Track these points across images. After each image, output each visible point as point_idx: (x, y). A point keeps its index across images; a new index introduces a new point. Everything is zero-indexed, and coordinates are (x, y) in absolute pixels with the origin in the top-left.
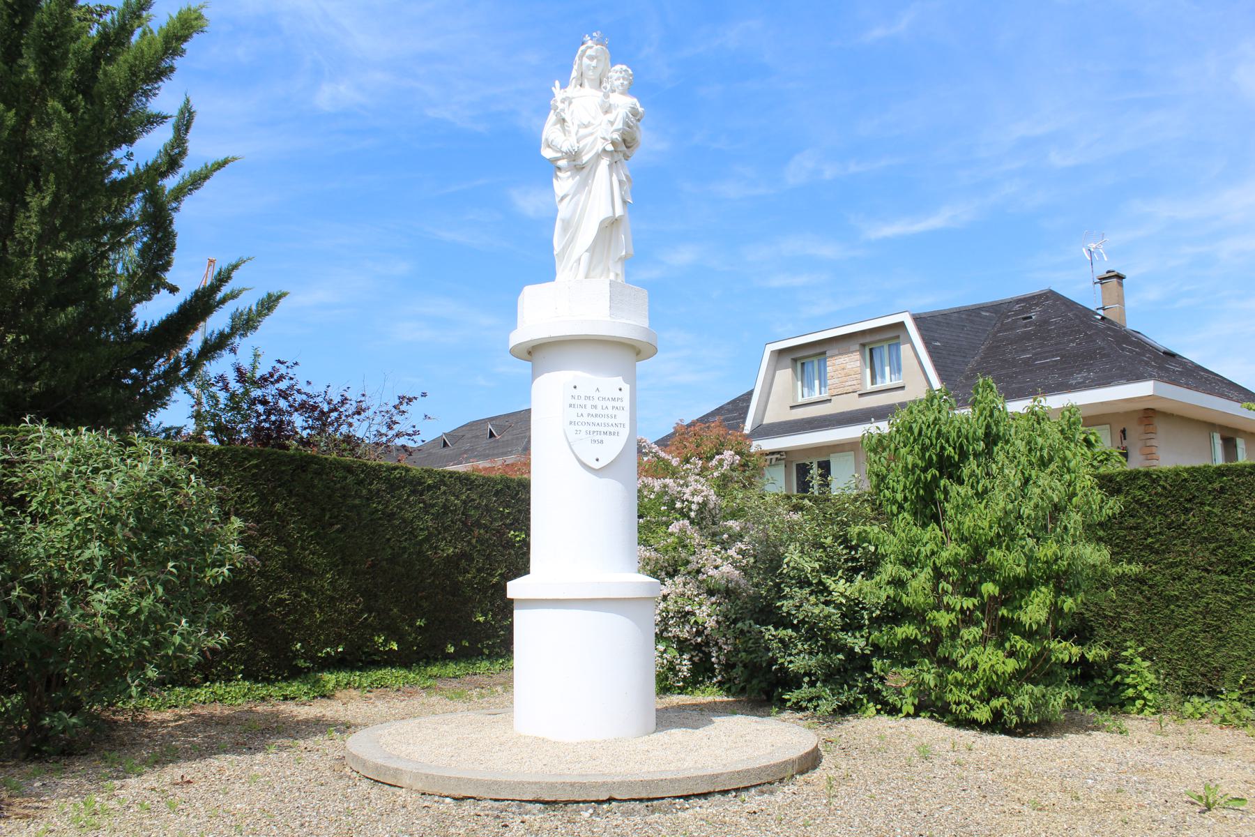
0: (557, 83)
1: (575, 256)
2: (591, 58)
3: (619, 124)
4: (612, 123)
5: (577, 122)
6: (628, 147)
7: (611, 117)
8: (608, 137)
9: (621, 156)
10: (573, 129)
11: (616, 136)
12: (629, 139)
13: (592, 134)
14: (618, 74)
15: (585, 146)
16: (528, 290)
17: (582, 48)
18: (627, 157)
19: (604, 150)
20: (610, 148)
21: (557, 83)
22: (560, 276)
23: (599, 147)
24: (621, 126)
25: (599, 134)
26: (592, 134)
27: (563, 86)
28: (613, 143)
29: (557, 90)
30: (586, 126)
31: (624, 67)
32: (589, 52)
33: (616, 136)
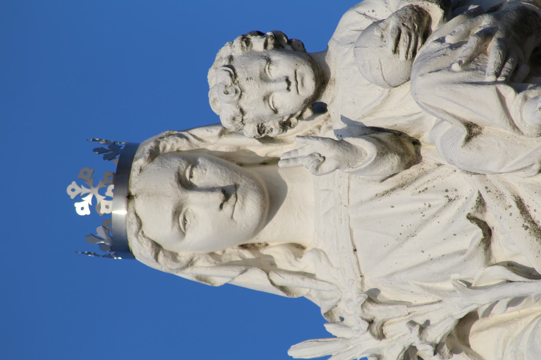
5: (477, 271)
14: (247, 88)
17: (141, 251)
24: (487, 94)
31: (216, 77)
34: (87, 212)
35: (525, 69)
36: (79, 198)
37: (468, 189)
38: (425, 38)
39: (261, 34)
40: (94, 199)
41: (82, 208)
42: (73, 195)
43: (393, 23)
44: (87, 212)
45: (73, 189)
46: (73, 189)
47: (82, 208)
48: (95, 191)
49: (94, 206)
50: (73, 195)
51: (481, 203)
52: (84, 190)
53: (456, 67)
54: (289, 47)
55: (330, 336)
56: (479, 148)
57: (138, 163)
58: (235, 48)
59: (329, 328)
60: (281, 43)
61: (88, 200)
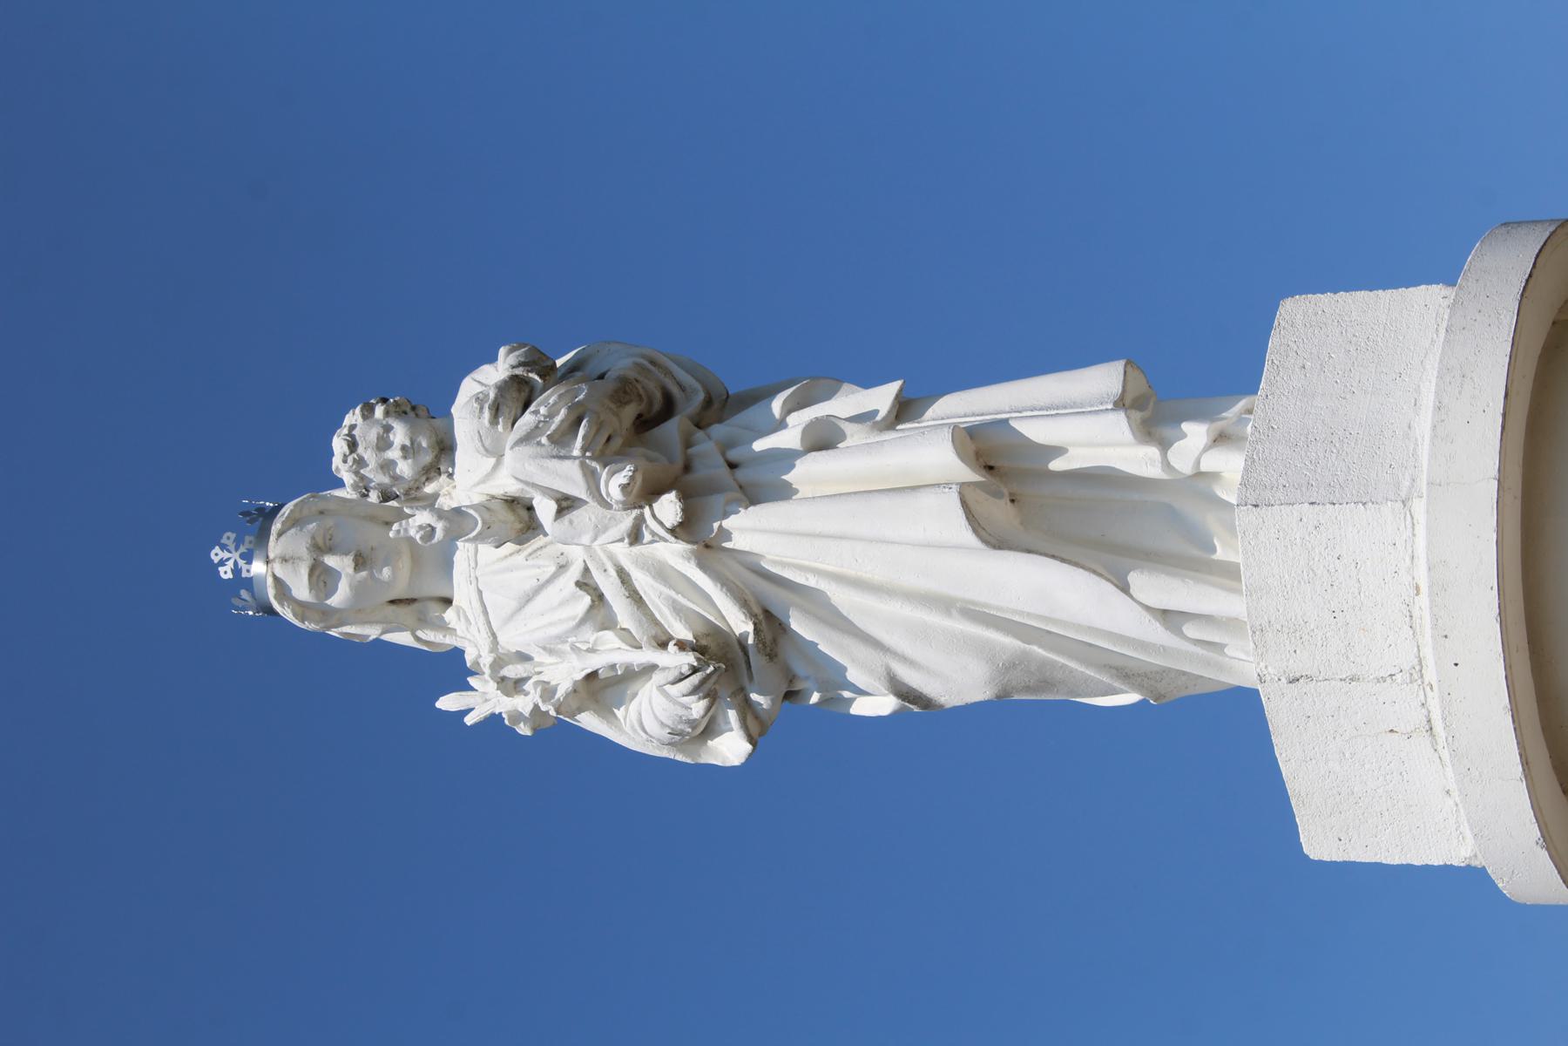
0: (448, 703)
1: (1156, 633)
2: (322, 578)
3: (568, 476)
4: (566, 504)
6: (668, 408)
7: (545, 509)
8: (627, 520)
9: (707, 446)
10: (611, 652)
11: (615, 483)
12: (630, 412)
13: (624, 577)
15: (678, 610)
16: (1323, 838)
17: (286, 613)
18: (720, 406)
19: (685, 529)
20: (669, 507)
21: (448, 703)
22: (1249, 681)
23: (674, 553)
25: (623, 552)
26: (624, 577)
27: (452, 669)
28: (649, 493)
29: (480, 701)
30: (599, 598)
31: (339, 445)
32: (301, 590)
33: (615, 483)
34: (230, 575)
35: (617, 443)
36: (222, 563)
37: (577, 555)
38: (526, 406)
39: (384, 401)
40: (236, 563)
41: (226, 573)
42: (216, 560)
43: (492, 396)
44: (230, 575)
45: (217, 554)
46: (217, 554)
47: (226, 573)
48: (236, 555)
49: (236, 570)
50: (216, 560)
51: (586, 570)
52: (226, 555)
53: (544, 440)
54: (412, 414)
55: (472, 689)
56: (571, 522)
57: (276, 526)
58: (353, 417)
59: (472, 681)
60: (399, 412)
61: (230, 564)
